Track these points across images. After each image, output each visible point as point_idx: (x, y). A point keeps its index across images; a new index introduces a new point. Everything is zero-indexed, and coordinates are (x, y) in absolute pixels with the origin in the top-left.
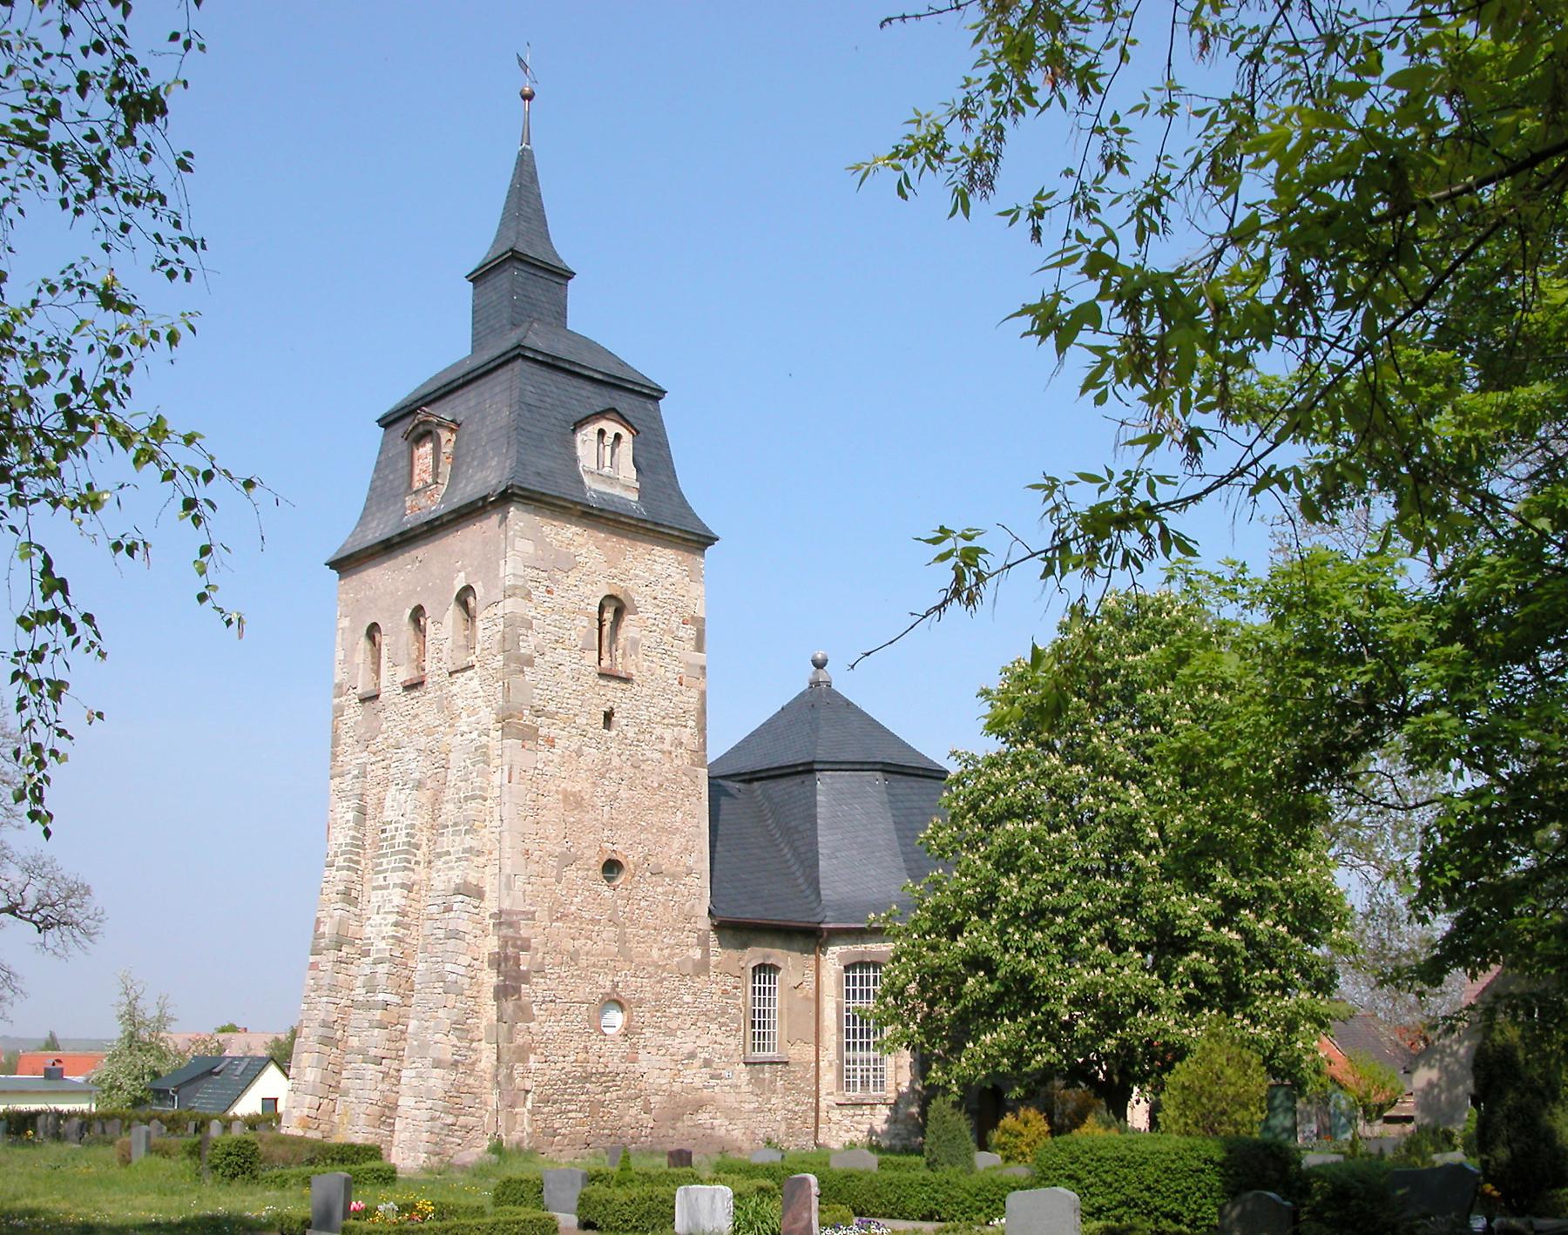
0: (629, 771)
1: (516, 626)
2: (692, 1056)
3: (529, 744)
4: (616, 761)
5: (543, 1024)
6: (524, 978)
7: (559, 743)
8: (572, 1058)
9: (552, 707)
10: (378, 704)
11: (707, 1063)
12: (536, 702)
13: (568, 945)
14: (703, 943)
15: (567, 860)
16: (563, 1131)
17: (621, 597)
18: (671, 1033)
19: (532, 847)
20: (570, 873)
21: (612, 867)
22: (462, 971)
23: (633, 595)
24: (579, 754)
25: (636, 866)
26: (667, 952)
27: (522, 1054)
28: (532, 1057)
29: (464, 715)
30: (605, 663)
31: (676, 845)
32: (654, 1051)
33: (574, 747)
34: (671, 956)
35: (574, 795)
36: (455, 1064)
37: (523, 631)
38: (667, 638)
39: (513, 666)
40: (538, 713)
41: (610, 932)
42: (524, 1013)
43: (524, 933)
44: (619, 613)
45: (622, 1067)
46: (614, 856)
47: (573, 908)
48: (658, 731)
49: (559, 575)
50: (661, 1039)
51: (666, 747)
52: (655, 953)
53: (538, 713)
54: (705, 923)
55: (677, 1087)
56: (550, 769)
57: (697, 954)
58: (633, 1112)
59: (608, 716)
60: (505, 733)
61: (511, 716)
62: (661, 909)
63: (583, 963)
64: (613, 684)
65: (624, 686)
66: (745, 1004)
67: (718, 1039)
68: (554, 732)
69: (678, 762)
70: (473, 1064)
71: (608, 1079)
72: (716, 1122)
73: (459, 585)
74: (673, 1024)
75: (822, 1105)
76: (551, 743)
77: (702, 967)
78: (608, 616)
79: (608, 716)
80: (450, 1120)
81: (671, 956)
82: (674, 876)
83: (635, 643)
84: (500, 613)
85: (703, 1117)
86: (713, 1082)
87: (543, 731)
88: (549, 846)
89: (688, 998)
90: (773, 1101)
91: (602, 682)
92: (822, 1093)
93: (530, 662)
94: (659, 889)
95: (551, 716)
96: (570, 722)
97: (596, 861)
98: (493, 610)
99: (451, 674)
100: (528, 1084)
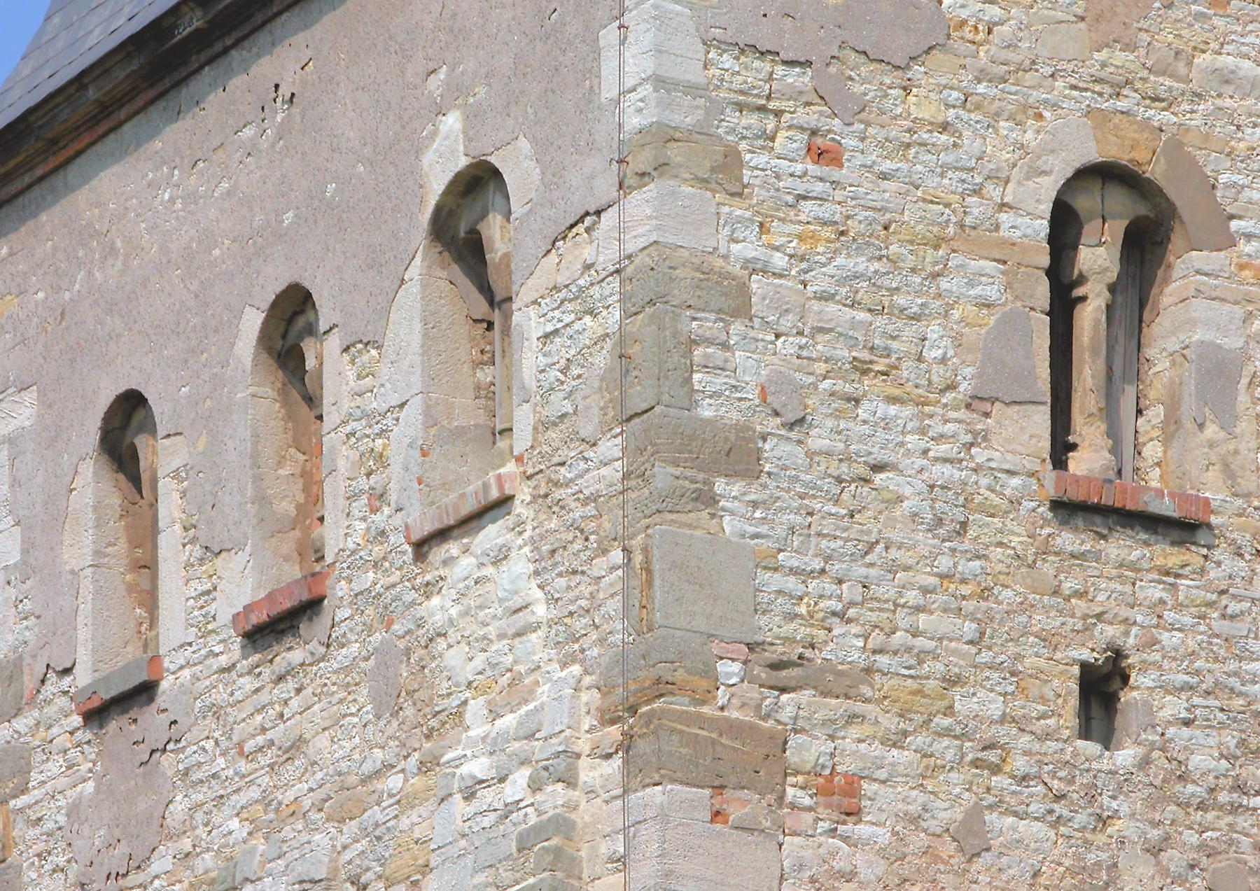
1: (676, 304)
9: (845, 647)
12: (771, 627)
17: (1156, 171)
23: (1211, 162)
24: (971, 839)
30: (1089, 460)
33: (946, 814)
37: (707, 325)
39: (663, 475)
40: (783, 671)
44: (1145, 246)
49: (866, 82)
53: (783, 671)
59: (1101, 689)
60: (639, 766)
64: (1123, 547)
65: (1172, 556)
68: (855, 750)
76: (843, 797)
78: (1098, 258)
79: (1101, 689)
83: (1219, 373)
87: (807, 750)
91: (1068, 540)
93: (740, 456)
95: (843, 684)
96: (924, 707)
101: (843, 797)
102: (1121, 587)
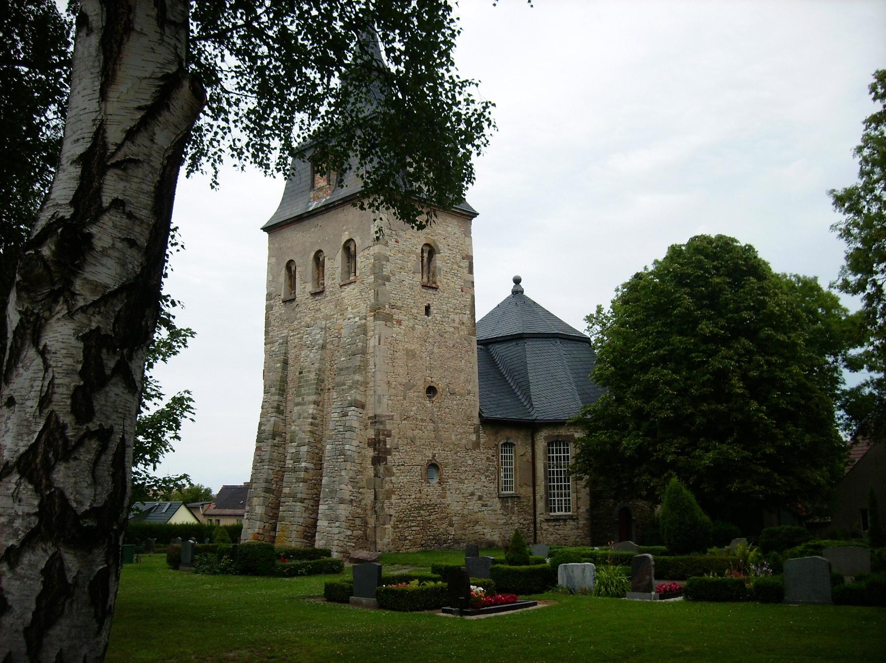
0: (437, 337)
1: (380, 260)
2: (472, 494)
3: (389, 324)
4: (432, 333)
5: (399, 478)
6: (388, 452)
7: (404, 323)
8: (413, 497)
9: (399, 304)
10: (295, 304)
11: (480, 498)
12: (392, 301)
13: (410, 433)
14: (476, 431)
15: (408, 386)
16: (409, 538)
18: (462, 482)
19: (391, 380)
20: (411, 394)
21: (431, 391)
22: (354, 449)
24: (413, 328)
25: (443, 390)
26: (459, 437)
27: (389, 494)
28: (394, 497)
29: (349, 308)
31: (462, 378)
32: (453, 491)
33: (411, 325)
34: (461, 439)
35: (411, 351)
36: (351, 501)
38: (455, 267)
39: (380, 281)
41: (431, 426)
42: (389, 472)
43: (388, 427)
45: (439, 501)
46: (432, 385)
47: (412, 413)
48: (452, 316)
50: (457, 485)
51: (456, 325)
52: (453, 437)
53: (393, 307)
54: (476, 421)
55: (466, 512)
56: (399, 337)
57: (474, 437)
58: (444, 526)
59: (428, 308)
60: (376, 318)
61: (379, 308)
62: (456, 413)
63: (418, 443)
66: (498, 465)
67: (486, 484)
68: (401, 317)
69: (462, 333)
70: (360, 501)
71: (431, 507)
72: (485, 531)
73: (345, 238)
74: (463, 477)
75: (538, 520)
76: (399, 322)
77: (476, 445)
78: (426, 255)
79: (428, 308)
80: (349, 533)
81: (461, 439)
82: (461, 395)
84: (372, 253)
85: (478, 528)
86: (484, 508)
88: (399, 379)
89: (470, 462)
90: (513, 518)
92: (538, 513)
93: (388, 280)
94: (455, 402)
95: (399, 308)
97: (422, 387)
98: (366, 252)
99: (341, 286)
100: (392, 512)
101: (399, 322)
102: (430, 297)
